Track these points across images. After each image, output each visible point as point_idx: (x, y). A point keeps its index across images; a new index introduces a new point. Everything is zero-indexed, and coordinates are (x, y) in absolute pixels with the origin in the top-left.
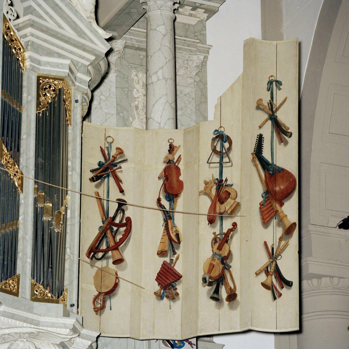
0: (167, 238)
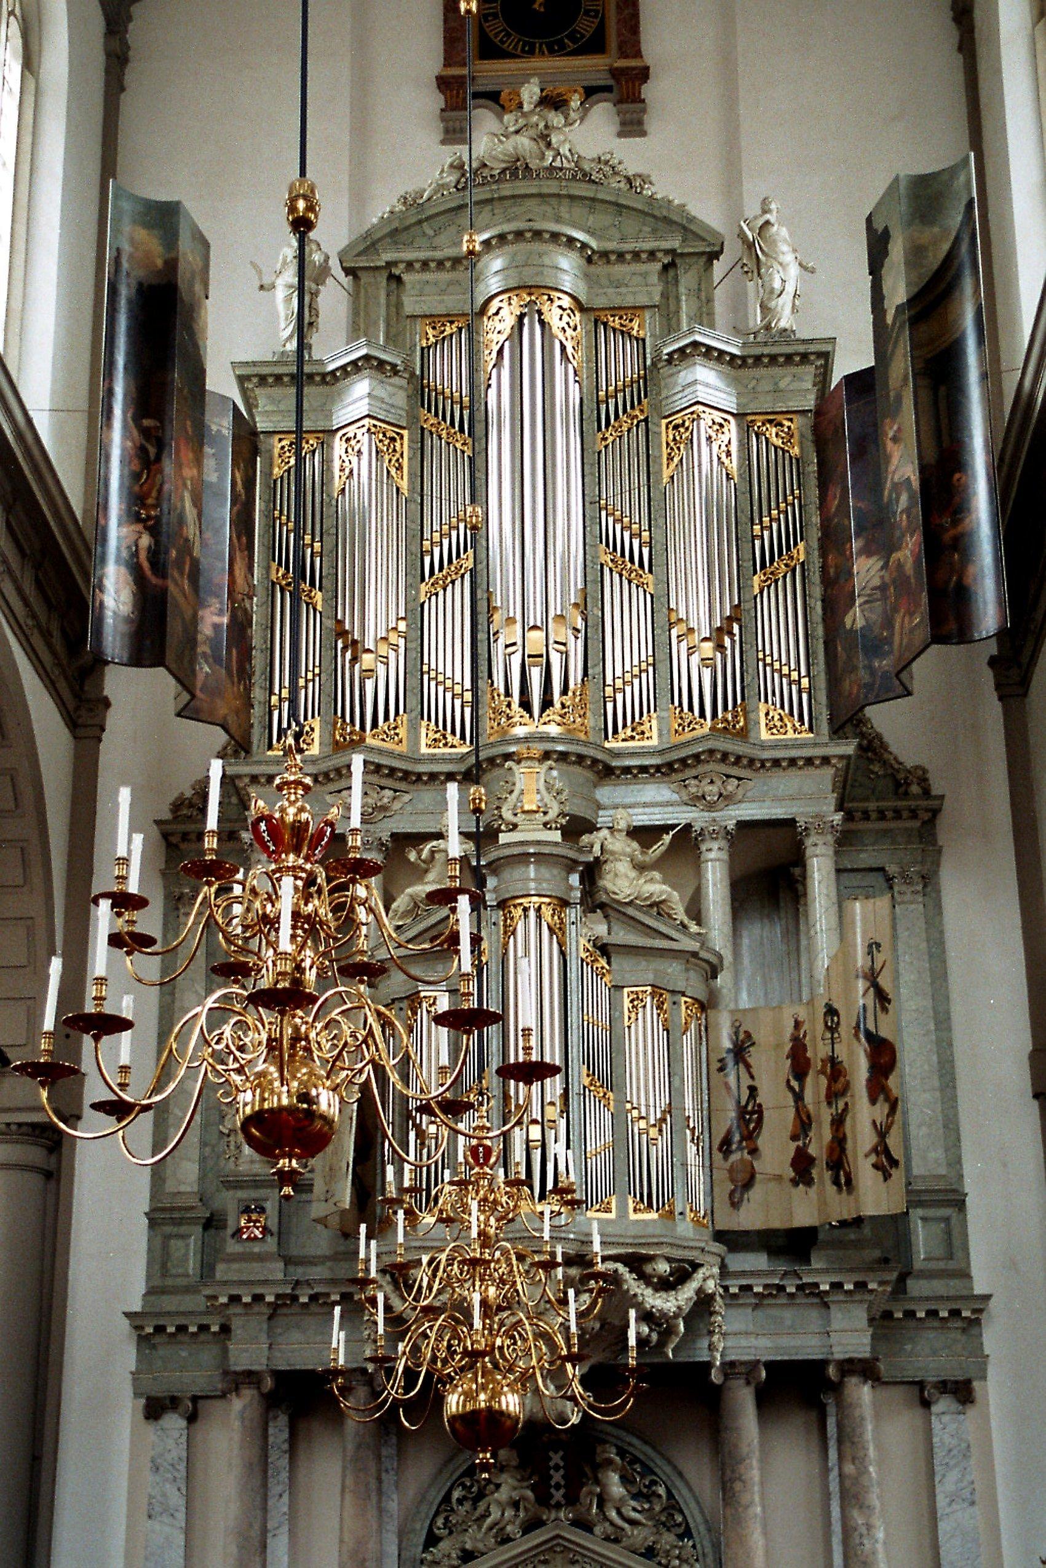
0: (798, 1122)
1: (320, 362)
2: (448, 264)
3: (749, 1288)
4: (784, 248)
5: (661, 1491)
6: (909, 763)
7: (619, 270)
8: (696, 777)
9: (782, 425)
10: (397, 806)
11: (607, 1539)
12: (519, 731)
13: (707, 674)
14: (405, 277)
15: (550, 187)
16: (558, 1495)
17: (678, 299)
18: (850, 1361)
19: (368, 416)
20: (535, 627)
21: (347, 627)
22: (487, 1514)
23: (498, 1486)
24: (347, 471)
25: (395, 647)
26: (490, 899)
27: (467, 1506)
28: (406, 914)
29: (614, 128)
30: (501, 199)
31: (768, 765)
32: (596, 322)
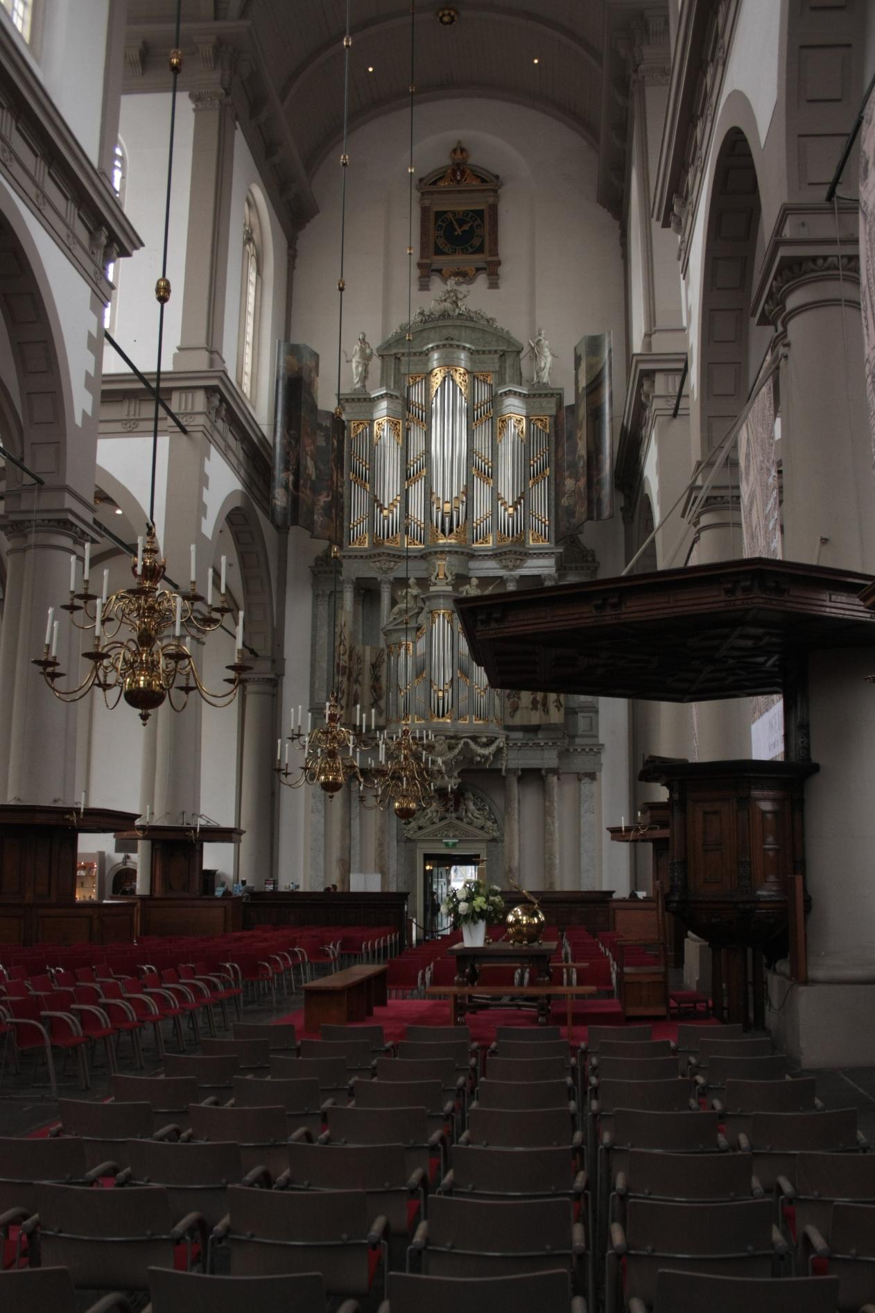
3: (516, 744)
4: (546, 350)
6: (588, 548)
7: (483, 357)
9: (542, 420)
10: (396, 567)
11: (468, 823)
12: (441, 541)
13: (511, 519)
15: (458, 323)
16: (452, 809)
17: (505, 368)
18: (550, 769)
20: (447, 502)
22: (427, 815)
25: (396, 507)
27: (421, 812)
28: (397, 614)
29: (486, 285)
30: (439, 327)
32: (474, 377)
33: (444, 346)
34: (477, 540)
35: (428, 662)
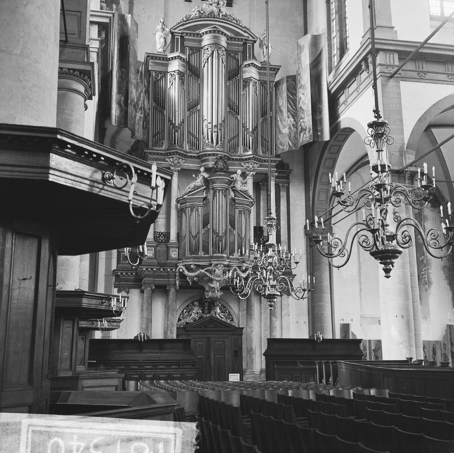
1: (167, 55)
2: (196, 35)
5: (227, 311)
8: (248, 163)
10: (182, 162)
14: (186, 37)
16: (206, 312)
19: (178, 70)
21: (171, 120)
23: (194, 309)
24: (171, 83)
26: (211, 188)
27: (187, 313)
31: (263, 161)
33: (214, 31)
34: (230, 150)
35: (211, 221)
